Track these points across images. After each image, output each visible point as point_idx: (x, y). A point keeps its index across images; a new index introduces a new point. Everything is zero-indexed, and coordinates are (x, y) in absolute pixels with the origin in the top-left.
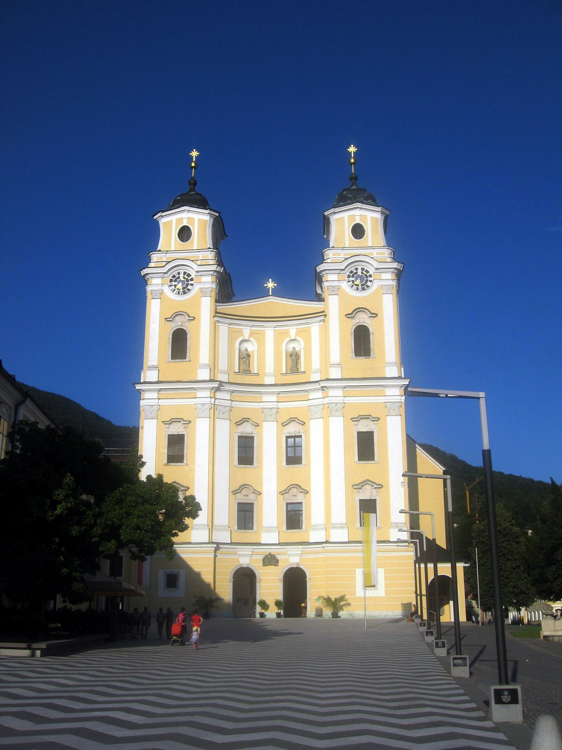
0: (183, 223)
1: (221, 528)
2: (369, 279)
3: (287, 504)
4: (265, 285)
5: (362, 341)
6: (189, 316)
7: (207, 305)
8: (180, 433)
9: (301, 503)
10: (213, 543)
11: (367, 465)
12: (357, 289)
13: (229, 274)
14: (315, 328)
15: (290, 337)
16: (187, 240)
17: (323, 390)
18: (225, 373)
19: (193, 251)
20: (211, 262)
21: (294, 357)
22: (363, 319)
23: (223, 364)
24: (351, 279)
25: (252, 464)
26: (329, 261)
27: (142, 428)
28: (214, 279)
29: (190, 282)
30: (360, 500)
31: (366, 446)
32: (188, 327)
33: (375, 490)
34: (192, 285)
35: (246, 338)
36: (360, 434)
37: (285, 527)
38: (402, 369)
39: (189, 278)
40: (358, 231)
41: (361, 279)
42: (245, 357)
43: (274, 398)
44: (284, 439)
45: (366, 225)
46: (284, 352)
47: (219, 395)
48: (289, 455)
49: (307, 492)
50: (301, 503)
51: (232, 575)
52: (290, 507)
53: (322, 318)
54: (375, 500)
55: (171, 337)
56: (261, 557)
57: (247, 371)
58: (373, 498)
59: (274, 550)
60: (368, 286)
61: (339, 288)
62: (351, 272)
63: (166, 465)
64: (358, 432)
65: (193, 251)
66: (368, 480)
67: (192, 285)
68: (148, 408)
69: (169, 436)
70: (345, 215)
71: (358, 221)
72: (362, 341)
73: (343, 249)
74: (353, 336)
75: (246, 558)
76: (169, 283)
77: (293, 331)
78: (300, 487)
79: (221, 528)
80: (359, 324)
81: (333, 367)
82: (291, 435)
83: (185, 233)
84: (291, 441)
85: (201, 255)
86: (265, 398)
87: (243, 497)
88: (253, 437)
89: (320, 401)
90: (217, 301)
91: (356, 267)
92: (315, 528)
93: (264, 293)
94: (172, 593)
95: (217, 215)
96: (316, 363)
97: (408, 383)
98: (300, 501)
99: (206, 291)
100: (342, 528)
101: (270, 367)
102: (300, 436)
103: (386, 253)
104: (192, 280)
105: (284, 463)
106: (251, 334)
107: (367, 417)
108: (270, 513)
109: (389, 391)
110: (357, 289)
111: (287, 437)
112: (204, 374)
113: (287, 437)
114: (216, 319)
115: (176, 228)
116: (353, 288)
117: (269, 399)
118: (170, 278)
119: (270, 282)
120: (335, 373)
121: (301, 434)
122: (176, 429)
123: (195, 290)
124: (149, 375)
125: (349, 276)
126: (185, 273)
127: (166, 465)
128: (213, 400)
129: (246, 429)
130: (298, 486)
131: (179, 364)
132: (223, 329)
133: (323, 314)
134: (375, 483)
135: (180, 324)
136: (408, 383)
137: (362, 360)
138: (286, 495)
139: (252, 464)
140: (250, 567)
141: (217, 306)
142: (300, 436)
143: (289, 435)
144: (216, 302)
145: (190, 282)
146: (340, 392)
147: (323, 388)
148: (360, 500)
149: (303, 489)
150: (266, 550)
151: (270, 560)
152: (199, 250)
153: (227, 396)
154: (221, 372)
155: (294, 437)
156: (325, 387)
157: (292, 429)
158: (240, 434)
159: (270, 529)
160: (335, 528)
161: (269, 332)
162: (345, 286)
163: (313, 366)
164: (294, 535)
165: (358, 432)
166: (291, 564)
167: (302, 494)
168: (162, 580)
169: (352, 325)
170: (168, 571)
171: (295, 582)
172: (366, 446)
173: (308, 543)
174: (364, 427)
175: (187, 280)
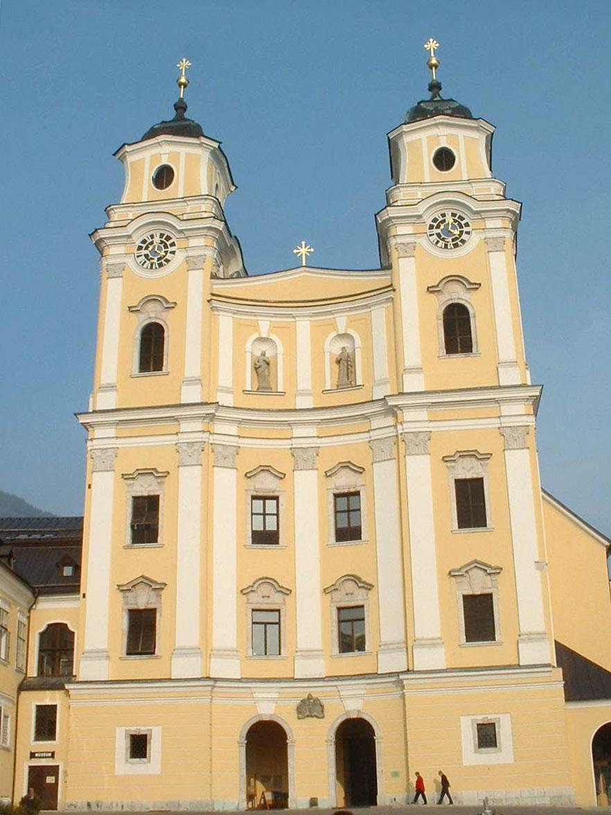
0: (161, 162)
1: (225, 653)
2: (465, 229)
3: (339, 609)
4: (295, 251)
5: (457, 329)
6: (167, 302)
7: (197, 285)
8: (152, 494)
9: (363, 606)
10: (209, 678)
11: (473, 535)
12: (446, 246)
13: (235, 237)
14: (379, 315)
15: (338, 331)
16: (168, 185)
17: (395, 415)
18: (228, 392)
19: (173, 200)
20: (205, 215)
21: (345, 363)
22: (457, 294)
23: (225, 377)
24: (435, 231)
25: (277, 543)
26: (396, 204)
27: (90, 487)
28: (210, 241)
29: (170, 249)
30: (464, 596)
31: (471, 504)
32: (169, 322)
33: (489, 577)
34: (173, 253)
35: (264, 335)
36: (461, 485)
37: (336, 650)
38: (528, 372)
39: (168, 243)
40: (444, 159)
41: (449, 231)
42: (262, 367)
43: (313, 431)
44: (331, 498)
45: (458, 150)
46: (327, 355)
47: (219, 427)
48: (339, 526)
49: (369, 587)
50: (363, 606)
51: (244, 734)
52: (346, 615)
53: (391, 295)
54: (490, 596)
55: (138, 336)
56: (298, 702)
57: (267, 388)
58: (487, 591)
59: (317, 691)
60: (463, 241)
61: (414, 246)
62: (435, 220)
63: (128, 547)
64: (456, 481)
65: (173, 200)
66: (476, 561)
67: (173, 253)
68: (98, 453)
69: (135, 498)
70: (423, 136)
71: (444, 144)
72: (457, 329)
73: (421, 184)
74: (442, 322)
75: (269, 704)
76: (136, 252)
77: (342, 322)
78: (359, 579)
79: (225, 653)
80: (451, 302)
81: (410, 373)
82: (342, 491)
83: (164, 177)
84: (343, 502)
85: (190, 208)
86: (297, 431)
87: (262, 600)
88: (276, 498)
89: (390, 432)
90: (214, 277)
91: (442, 212)
92: (387, 647)
93: (294, 264)
94: (139, 766)
95: (216, 145)
96: (382, 369)
97: (538, 394)
98: (361, 603)
99: (195, 260)
100: (434, 645)
101: (305, 380)
102: (357, 494)
103: (492, 189)
104: (173, 244)
105: (333, 539)
106: (274, 328)
107: (473, 454)
108: (311, 625)
109: (506, 409)
110: (446, 246)
111: (336, 496)
112: (191, 394)
113: (336, 496)
114: (215, 304)
115: (151, 169)
116: (439, 245)
117: (305, 434)
118: (138, 243)
119: (303, 246)
120: (413, 383)
121: (358, 489)
122: (145, 488)
123: (178, 260)
124: (104, 400)
125: (431, 227)
126: (162, 236)
127: (128, 547)
128: (206, 435)
129: (266, 484)
130: (355, 579)
131: (152, 380)
132: (226, 322)
133: (391, 287)
134: (489, 566)
135: (153, 315)
136: (538, 394)
137: (459, 359)
138: (335, 594)
139: (277, 543)
140: (275, 719)
141: (213, 284)
142: (357, 494)
143: (338, 492)
144: (211, 278)
145: (170, 249)
146: (423, 414)
147: (392, 411)
148: (464, 596)
149: (363, 582)
150: (302, 692)
151: (310, 708)
152: (184, 199)
153: (233, 429)
154: (222, 391)
155: (348, 495)
156: (396, 406)
157: (345, 481)
158: (255, 494)
159: (308, 654)
160: (423, 646)
161: (304, 326)
162: (423, 242)
163: (375, 375)
164: (353, 662)
165: (456, 481)
166: (347, 712)
167: (364, 591)
168: (122, 745)
169: (437, 307)
170: (134, 730)
171: (355, 744)
172: (471, 504)
173: (376, 675)
174: (467, 471)
175: (166, 247)
